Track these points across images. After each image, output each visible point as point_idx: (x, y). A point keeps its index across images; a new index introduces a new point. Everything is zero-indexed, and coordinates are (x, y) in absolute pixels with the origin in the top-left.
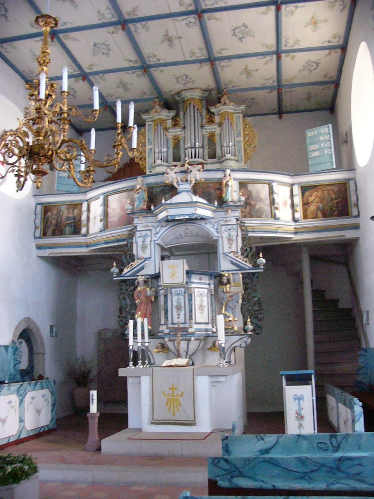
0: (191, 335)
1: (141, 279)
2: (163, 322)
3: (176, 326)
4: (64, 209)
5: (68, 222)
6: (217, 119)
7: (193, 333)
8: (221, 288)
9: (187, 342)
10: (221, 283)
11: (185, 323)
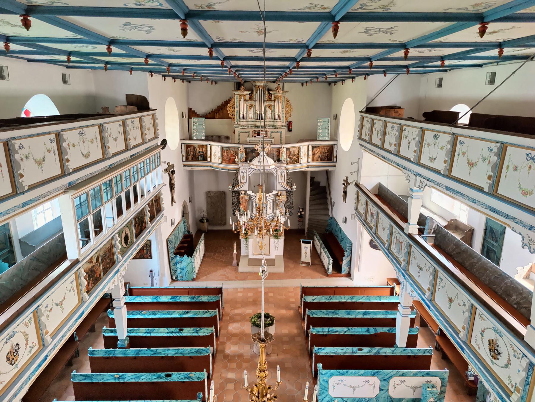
4: (197, 147)
6: (273, 98)
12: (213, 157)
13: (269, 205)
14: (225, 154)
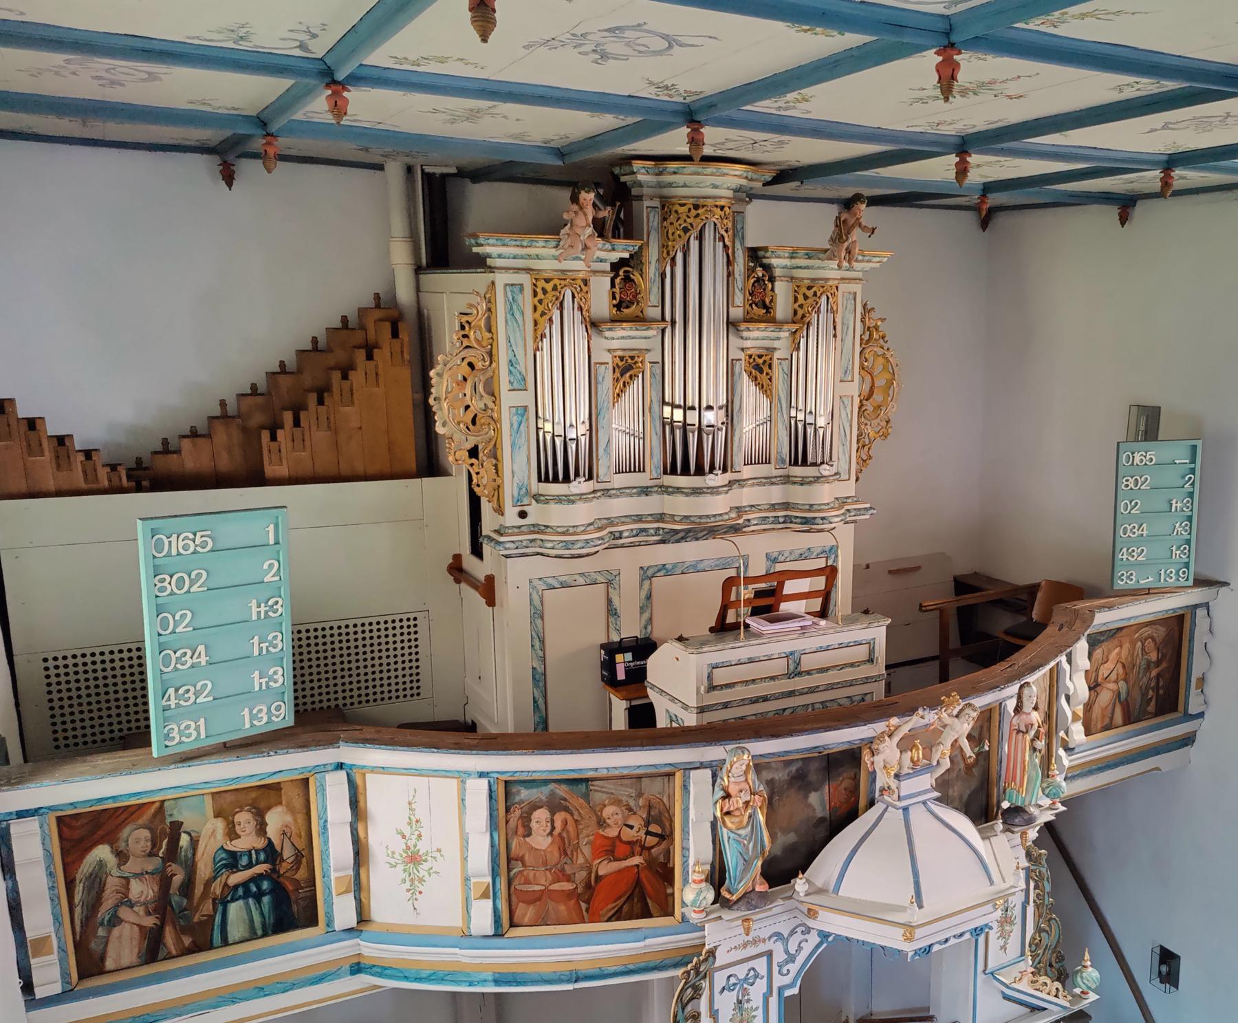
5: (236, 878)
12: (385, 885)
14: (541, 840)
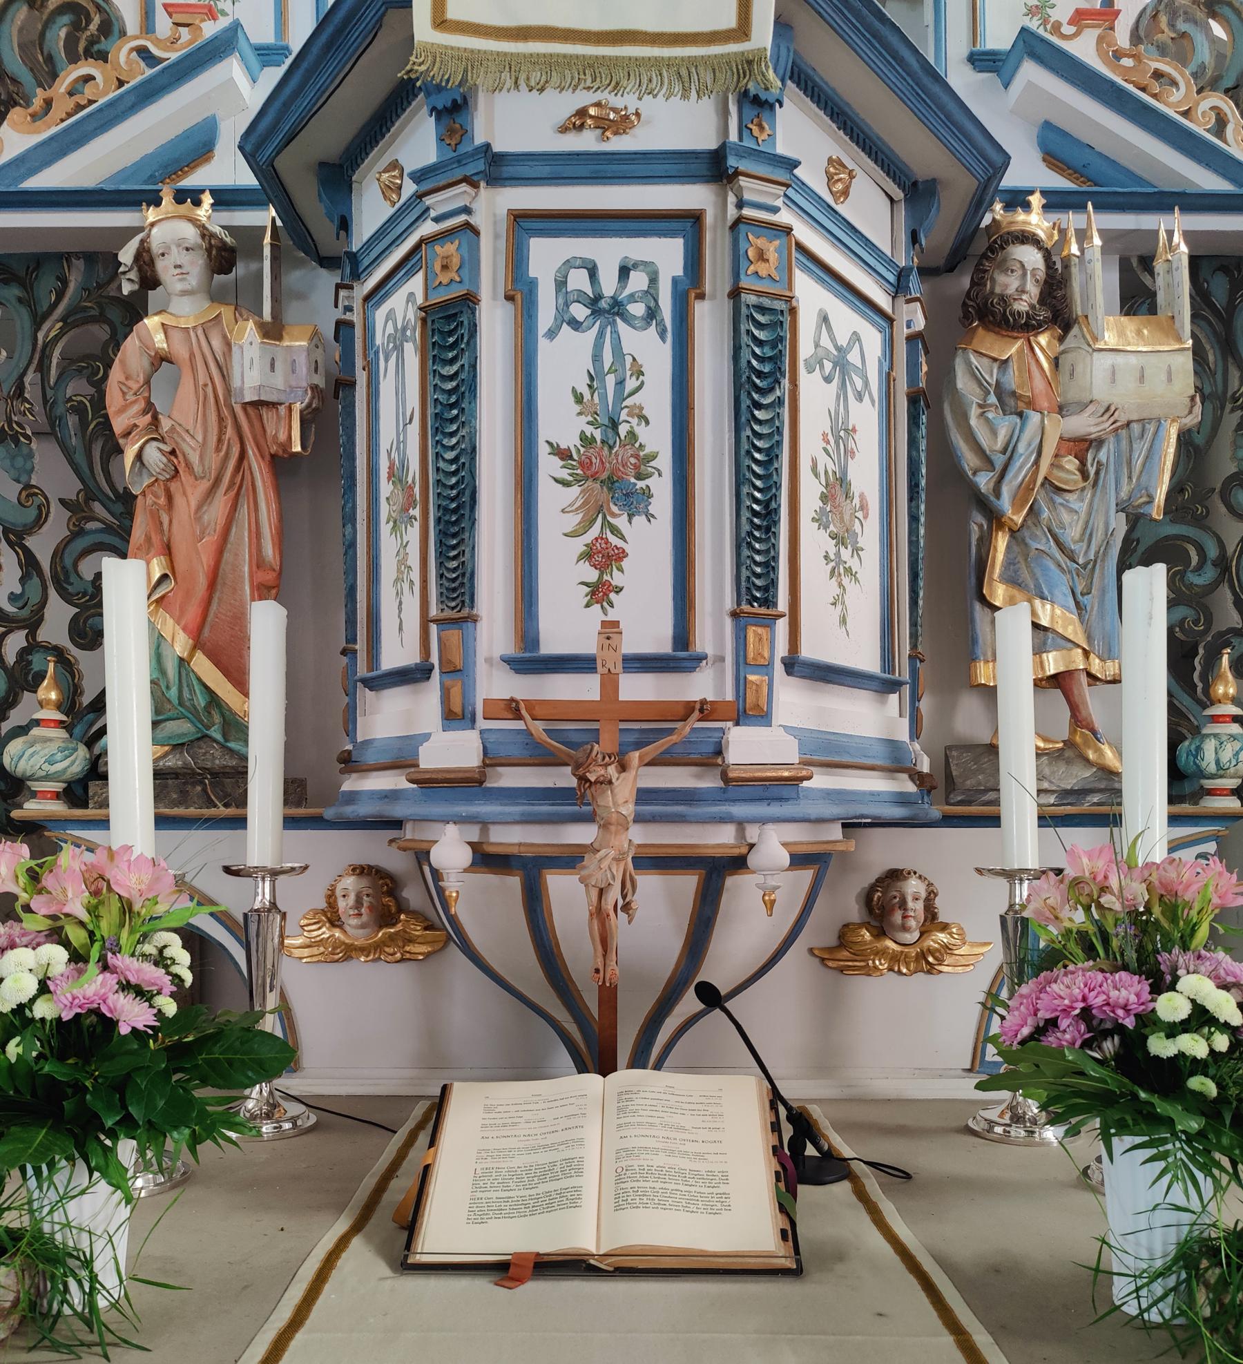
0: (739, 810)
1: (171, 232)
2: (398, 650)
3: (580, 688)
7: (774, 788)
8: (983, 361)
9: (688, 883)
10: (988, 314)
11: (680, 657)
13: (815, 396)
